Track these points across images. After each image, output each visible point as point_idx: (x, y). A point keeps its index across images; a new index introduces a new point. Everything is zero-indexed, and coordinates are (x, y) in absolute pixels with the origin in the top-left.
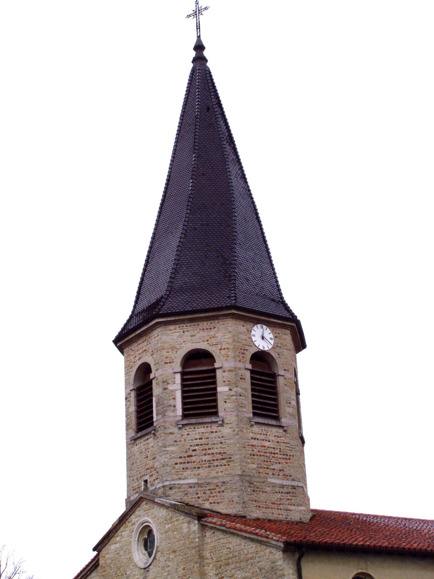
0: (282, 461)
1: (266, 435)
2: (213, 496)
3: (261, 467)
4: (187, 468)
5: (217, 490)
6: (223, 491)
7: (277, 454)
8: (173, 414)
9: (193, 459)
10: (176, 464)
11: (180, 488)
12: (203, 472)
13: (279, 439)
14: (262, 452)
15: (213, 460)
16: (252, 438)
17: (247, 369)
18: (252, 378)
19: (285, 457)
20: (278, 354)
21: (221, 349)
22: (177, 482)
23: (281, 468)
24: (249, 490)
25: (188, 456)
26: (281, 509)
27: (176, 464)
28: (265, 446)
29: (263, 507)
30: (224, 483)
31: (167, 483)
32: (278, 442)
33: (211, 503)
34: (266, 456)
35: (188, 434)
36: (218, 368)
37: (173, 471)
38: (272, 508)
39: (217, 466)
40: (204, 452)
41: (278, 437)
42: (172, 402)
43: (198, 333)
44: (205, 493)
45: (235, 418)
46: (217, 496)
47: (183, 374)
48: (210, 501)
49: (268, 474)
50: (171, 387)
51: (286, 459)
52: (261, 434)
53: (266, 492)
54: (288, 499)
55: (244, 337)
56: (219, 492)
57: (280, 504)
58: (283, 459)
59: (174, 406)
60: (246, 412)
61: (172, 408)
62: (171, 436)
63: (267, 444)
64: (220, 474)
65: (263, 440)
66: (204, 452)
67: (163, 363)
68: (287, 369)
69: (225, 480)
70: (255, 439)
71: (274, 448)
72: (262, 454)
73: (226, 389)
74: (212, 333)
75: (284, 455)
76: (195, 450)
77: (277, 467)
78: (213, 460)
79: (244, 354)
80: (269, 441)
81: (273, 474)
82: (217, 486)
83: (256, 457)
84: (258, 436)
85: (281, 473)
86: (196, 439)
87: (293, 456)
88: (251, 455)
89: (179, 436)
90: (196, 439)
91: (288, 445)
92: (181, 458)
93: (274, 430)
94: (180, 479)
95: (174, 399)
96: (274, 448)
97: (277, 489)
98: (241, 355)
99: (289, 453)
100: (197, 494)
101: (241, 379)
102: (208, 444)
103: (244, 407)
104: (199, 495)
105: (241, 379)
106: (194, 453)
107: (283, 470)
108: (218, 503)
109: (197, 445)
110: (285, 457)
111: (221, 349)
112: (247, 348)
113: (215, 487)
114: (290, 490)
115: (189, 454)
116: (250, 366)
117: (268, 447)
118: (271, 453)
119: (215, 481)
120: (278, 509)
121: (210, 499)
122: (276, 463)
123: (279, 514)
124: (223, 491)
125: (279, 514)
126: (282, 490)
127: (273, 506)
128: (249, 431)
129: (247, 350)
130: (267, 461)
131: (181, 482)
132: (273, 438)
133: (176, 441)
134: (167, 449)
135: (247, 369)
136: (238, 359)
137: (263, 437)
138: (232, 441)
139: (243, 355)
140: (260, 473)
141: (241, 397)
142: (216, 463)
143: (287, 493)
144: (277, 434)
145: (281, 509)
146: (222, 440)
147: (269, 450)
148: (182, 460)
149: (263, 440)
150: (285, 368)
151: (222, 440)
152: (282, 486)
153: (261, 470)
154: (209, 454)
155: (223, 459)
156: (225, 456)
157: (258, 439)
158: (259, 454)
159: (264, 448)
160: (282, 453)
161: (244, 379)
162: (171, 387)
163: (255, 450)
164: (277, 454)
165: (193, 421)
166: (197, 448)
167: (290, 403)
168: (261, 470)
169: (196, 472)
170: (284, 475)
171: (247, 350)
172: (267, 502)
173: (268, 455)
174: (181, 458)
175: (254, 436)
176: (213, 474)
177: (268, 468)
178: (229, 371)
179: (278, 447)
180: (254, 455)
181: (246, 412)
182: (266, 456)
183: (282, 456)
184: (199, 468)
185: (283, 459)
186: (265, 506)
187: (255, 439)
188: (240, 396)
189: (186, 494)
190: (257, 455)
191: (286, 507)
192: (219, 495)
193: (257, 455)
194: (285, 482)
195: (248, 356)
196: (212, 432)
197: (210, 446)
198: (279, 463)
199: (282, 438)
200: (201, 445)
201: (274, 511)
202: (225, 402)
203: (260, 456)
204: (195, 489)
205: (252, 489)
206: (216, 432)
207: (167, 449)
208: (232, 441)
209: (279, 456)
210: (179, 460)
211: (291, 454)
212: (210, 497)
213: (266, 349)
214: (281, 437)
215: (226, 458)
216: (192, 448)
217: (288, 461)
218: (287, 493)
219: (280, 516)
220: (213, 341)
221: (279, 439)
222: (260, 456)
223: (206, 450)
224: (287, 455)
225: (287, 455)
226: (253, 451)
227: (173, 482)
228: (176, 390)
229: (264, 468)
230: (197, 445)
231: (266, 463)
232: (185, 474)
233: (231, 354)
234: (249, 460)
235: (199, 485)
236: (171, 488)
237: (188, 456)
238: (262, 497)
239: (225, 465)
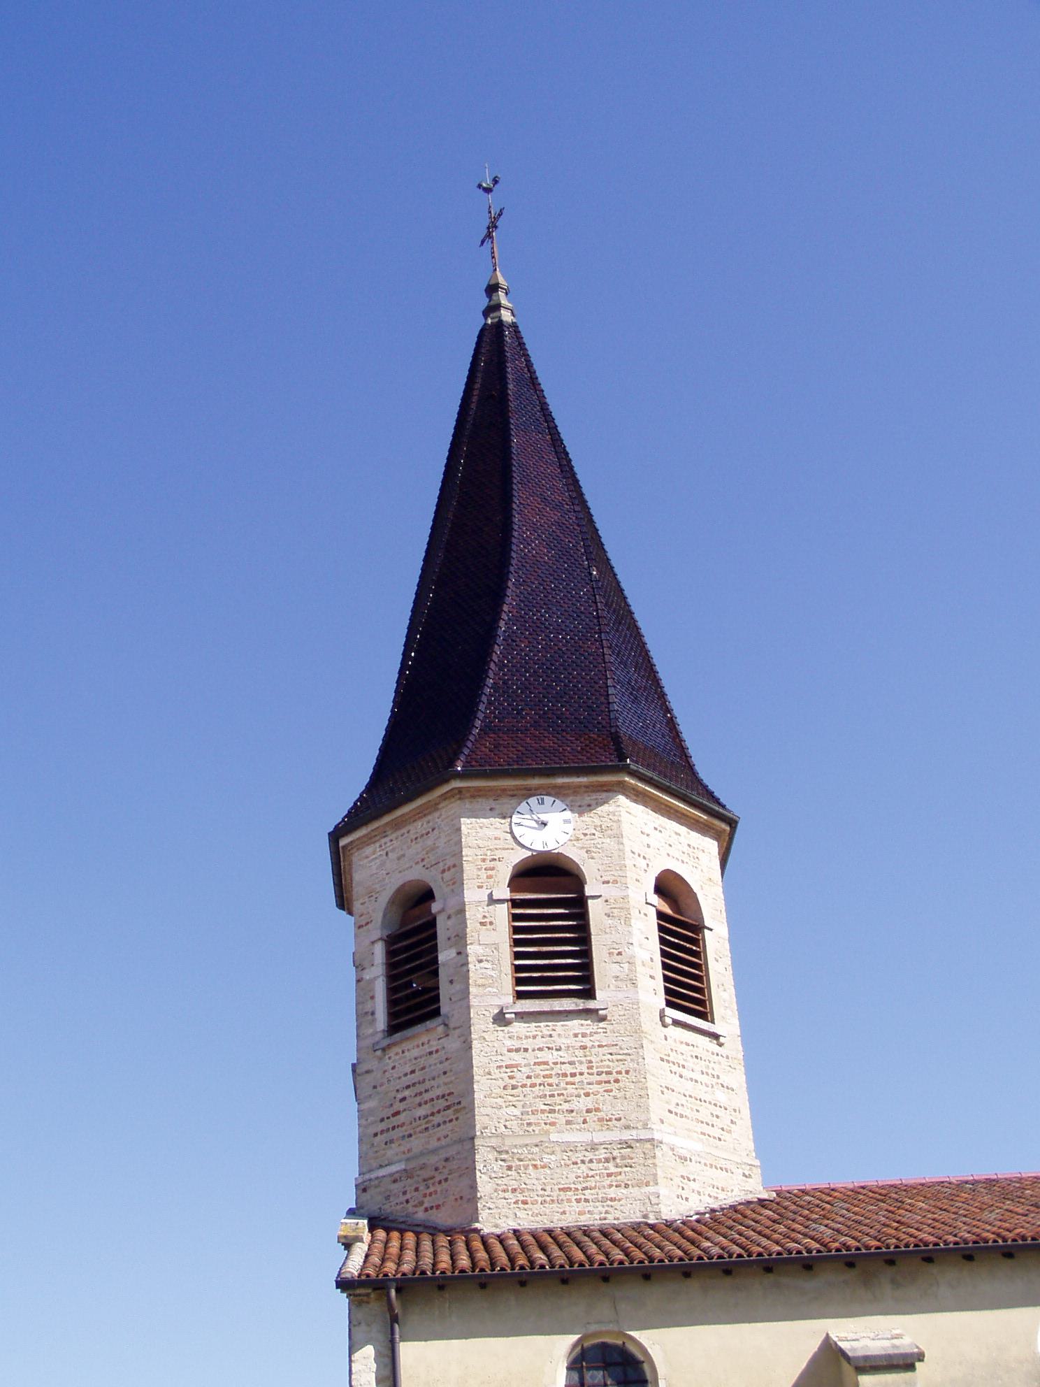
0: (595, 1088)
1: (551, 1036)
2: (431, 1194)
4: (392, 1141)
6: (446, 1180)
7: (581, 1074)
8: (371, 1031)
10: (376, 1135)
12: (416, 1144)
14: (537, 1076)
19: (604, 1077)
21: (443, 871)
22: (373, 1175)
23: (590, 1106)
26: (587, 1201)
27: (376, 1135)
28: (546, 1063)
30: (447, 1160)
32: (584, 1048)
33: (426, 1210)
34: (550, 1085)
35: (393, 1068)
36: (439, 912)
39: (439, 1125)
40: (418, 1099)
41: (584, 1035)
43: (409, 848)
46: (436, 1192)
48: (426, 1205)
51: (609, 1082)
52: (534, 1037)
54: (609, 1175)
56: (440, 1182)
57: (585, 1189)
58: (599, 1083)
59: (373, 1013)
61: (370, 1017)
64: (443, 1142)
69: (448, 1155)
70: (518, 1050)
71: (571, 1063)
75: (599, 1074)
76: (403, 1099)
77: (582, 1104)
78: (433, 1114)
79: (493, 869)
80: (559, 1050)
82: (436, 1169)
85: (590, 1117)
86: (406, 1075)
87: (627, 1072)
88: (505, 1088)
90: (406, 1075)
91: (613, 1050)
94: (381, 1166)
95: (372, 998)
96: (571, 1063)
98: (483, 874)
99: (615, 1067)
100: (405, 1193)
101: (482, 924)
102: (424, 1081)
104: (408, 1196)
105: (482, 924)
107: (597, 1110)
108: (438, 1207)
109: (408, 1087)
110: (604, 1077)
111: (443, 871)
112: (498, 854)
113: (433, 1173)
117: (556, 1063)
118: (565, 1075)
119: (433, 1160)
121: (426, 1200)
122: (579, 1096)
123: (581, 1213)
124: (446, 1180)
126: (590, 1155)
130: (552, 1096)
131: (382, 1172)
132: (571, 1041)
133: (375, 1087)
137: (540, 1042)
139: (490, 872)
141: (484, 964)
142: (437, 1119)
145: (587, 1201)
147: (557, 1069)
150: (605, 878)
152: (593, 1147)
153: (532, 1119)
154: (426, 1103)
155: (448, 1107)
156: (451, 1100)
157: (526, 1050)
159: (542, 1067)
160: (595, 1070)
161: (491, 923)
163: (518, 1075)
164: (581, 1074)
166: (407, 1093)
167: (620, 954)
168: (532, 1119)
169: (406, 1145)
170: (601, 1120)
172: (548, 1188)
174: (382, 1120)
175: (517, 1044)
176: (434, 1144)
179: (583, 1059)
180: (514, 1087)
182: (550, 1085)
184: (410, 1136)
185: (599, 1083)
186: (540, 1199)
187: (518, 1050)
190: (524, 1086)
192: (439, 1188)
194: (599, 1137)
196: (431, 1053)
197: (427, 1085)
198: (587, 1095)
199: (596, 1037)
200: (414, 1084)
202: (451, 982)
206: (437, 1051)
209: (586, 1078)
211: (623, 1068)
212: (425, 1195)
216: (400, 1096)
217: (613, 1086)
219: (583, 1218)
222: (533, 1085)
223: (421, 1094)
224: (609, 1073)
225: (609, 1073)
228: (375, 978)
229: (543, 1111)
230: (408, 1087)
231: (548, 1100)
232: (390, 1153)
238: (533, 1178)
239: (451, 1121)
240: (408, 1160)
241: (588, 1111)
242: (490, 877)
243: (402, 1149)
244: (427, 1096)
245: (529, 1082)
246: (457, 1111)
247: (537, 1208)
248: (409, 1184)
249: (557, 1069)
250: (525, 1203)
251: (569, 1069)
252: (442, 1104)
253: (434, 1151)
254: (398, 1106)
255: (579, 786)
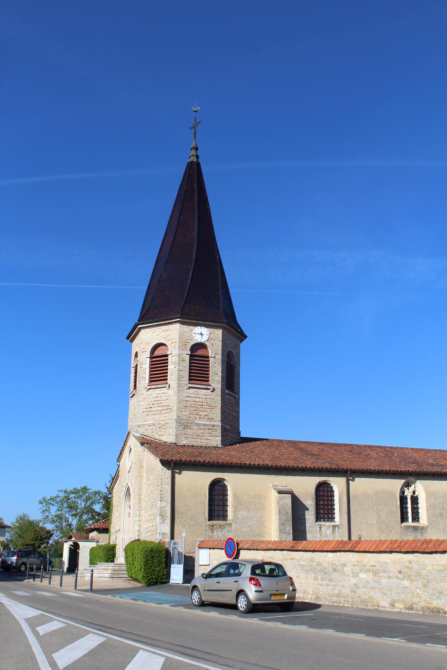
0: (208, 410)
3: (192, 414)
4: (149, 415)
5: (163, 428)
8: (144, 383)
9: (152, 409)
10: (143, 412)
11: (144, 426)
13: (207, 397)
15: (163, 410)
16: (187, 397)
17: (187, 354)
18: (190, 360)
19: (210, 407)
20: (212, 344)
21: (172, 343)
22: (142, 423)
24: (181, 427)
25: (150, 408)
27: (143, 412)
28: (196, 401)
29: (190, 438)
30: (166, 423)
31: (138, 423)
32: (206, 398)
33: (159, 435)
37: (141, 416)
38: (196, 439)
40: (158, 405)
41: (206, 395)
42: (144, 375)
43: (161, 333)
44: (156, 429)
45: (176, 385)
47: (151, 358)
49: (196, 418)
50: (144, 366)
53: (193, 429)
54: (209, 433)
55: (188, 335)
58: (209, 408)
60: (184, 381)
62: (142, 396)
63: (197, 400)
65: (195, 397)
66: (158, 405)
67: (141, 352)
68: (217, 353)
70: (189, 397)
71: (202, 402)
72: (193, 406)
73: (173, 367)
74: (168, 333)
76: (153, 404)
78: (163, 410)
80: (199, 398)
81: (200, 418)
83: (188, 408)
84: (192, 395)
85: (206, 417)
89: (146, 396)
91: (213, 400)
92: (146, 408)
93: (204, 391)
94: (144, 421)
95: (145, 373)
96: (202, 402)
97: (201, 427)
98: (184, 346)
99: (213, 405)
100: (152, 430)
103: (183, 378)
104: (153, 431)
106: (153, 406)
107: (208, 416)
108: (163, 435)
109: (155, 401)
110: (210, 407)
111: (172, 343)
112: (189, 341)
114: (211, 428)
115: (150, 406)
116: (189, 353)
118: (200, 405)
119: (162, 422)
120: (201, 439)
125: (201, 442)
127: (197, 437)
128: (184, 392)
129: (189, 343)
131: (145, 423)
132: (203, 396)
134: (139, 403)
135: (187, 354)
136: (181, 348)
137: (194, 395)
138: (173, 399)
140: (190, 417)
142: (164, 412)
143: (209, 429)
144: (205, 394)
146: (168, 398)
147: (199, 403)
148: (146, 410)
149: (195, 397)
151: (168, 398)
153: (191, 416)
155: (167, 409)
156: (169, 407)
158: (191, 406)
162: (144, 366)
163: (188, 404)
165: (153, 387)
166: (154, 402)
168: (191, 416)
169: (153, 417)
170: (208, 418)
171: (189, 343)
173: (197, 406)
174: (146, 408)
175: (189, 395)
176: (162, 418)
177: (196, 414)
178: (176, 356)
180: (187, 407)
181: (184, 381)
183: (208, 407)
185: (209, 408)
187: (189, 397)
188: (181, 371)
189: (146, 430)
190: (189, 407)
191: (207, 438)
192: (163, 430)
193: (189, 407)
195: (189, 346)
197: (162, 402)
198: (205, 411)
201: (197, 440)
203: (192, 407)
204: (151, 427)
205: (183, 427)
207: (139, 403)
208: (173, 399)
210: (145, 410)
213: (203, 341)
214: (208, 395)
215: (169, 409)
216: (152, 403)
218: (209, 429)
220: (168, 338)
221: (207, 397)
222: (192, 407)
224: (211, 406)
225: (211, 406)
226: (186, 404)
227: (140, 423)
228: (146, 368)
229: (194, 414)
230: (155, 401)
231: (196, 411)
233: (177, 345)
234: (183, 410)
235: (154, 425)
236: (139, 427)
237: (150, 408)
238: (190, 431)
240: (154, 421)
241: (205, 416)
242: (185, 347)
243: (152, 417)
244: (161, 405)
245: (191, 406)
246: (171, 411)
247: (190, 440)
248: (154, 428)
249: (199, 403)
250: (187, 438)
251: (201, 404)
252: (166, 408)
253: (163, 420)
254: (151, 406)
255: (212, 325)
